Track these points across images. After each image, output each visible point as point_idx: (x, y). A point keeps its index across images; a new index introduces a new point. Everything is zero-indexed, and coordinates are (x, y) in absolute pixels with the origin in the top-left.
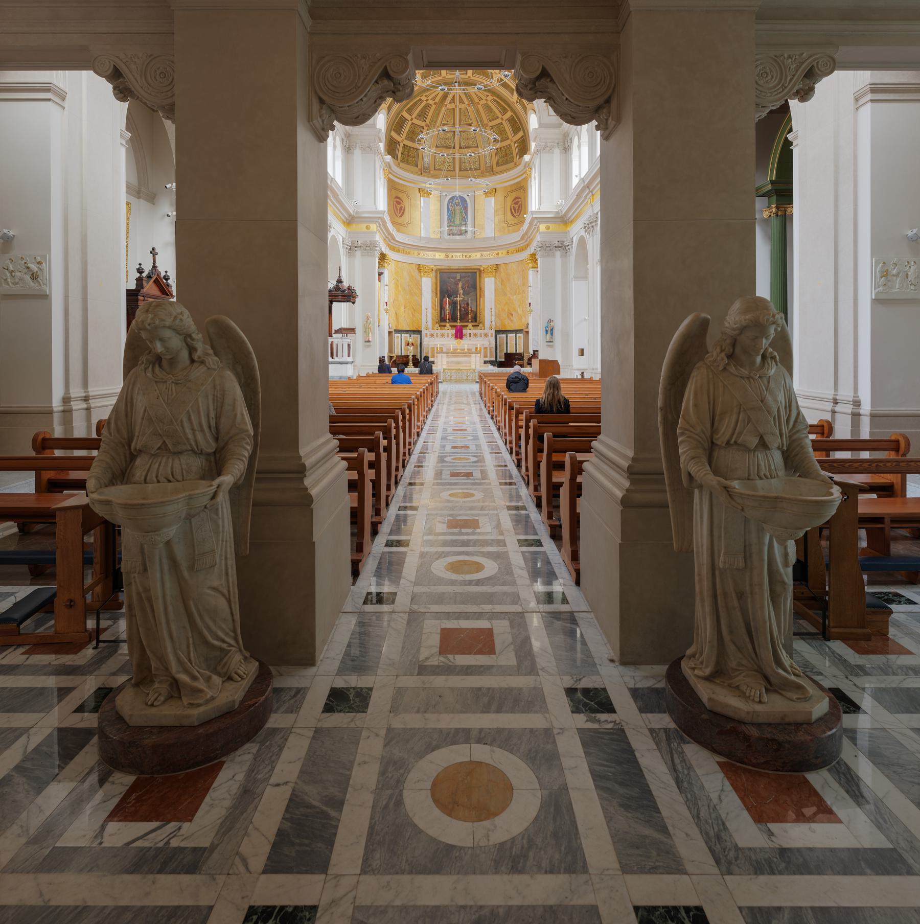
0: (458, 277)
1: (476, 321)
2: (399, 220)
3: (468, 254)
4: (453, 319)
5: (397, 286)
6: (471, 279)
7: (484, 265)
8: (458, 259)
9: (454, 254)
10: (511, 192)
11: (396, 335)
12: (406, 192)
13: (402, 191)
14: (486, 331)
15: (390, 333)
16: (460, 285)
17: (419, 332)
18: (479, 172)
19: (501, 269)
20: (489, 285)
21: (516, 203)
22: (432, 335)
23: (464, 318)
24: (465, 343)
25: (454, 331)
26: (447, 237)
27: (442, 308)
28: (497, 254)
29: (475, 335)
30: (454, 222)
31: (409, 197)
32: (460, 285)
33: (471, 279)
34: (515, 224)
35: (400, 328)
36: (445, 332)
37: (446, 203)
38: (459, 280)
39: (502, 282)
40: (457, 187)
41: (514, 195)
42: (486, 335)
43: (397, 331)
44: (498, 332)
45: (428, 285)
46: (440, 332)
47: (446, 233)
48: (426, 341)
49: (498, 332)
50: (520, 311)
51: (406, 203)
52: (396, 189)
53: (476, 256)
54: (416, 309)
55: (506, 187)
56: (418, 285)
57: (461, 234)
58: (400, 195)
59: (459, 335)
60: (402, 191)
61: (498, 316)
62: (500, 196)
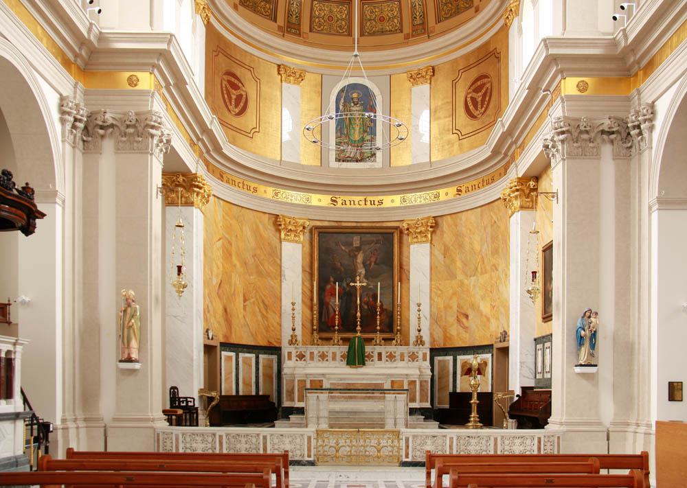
0: (356, 241)
1: (391, 330)
2: (235, 121)
3: (377, 198)
4: (348, 324)
5: (227, 254)
6: (384, 245)
7: (410, 218)
8: (356, 210)
9: (347, 198)
10: (468, 68)
12: (250, 69)
13: (242, 64)
14: (412, 348)
15: (209, 349)
16: (360, 259)
17: (275, 350)
18: (401, 35)
19: (445, 225)
20: (419, 258)
21: (477, 90)
22: (301, 357)
23: (368, 325)
24: (374, 371)
25: (345, 349)
26: (334, 164)
27: (322, 304)
28: (437, 196)
29: (391, 357)
30: (348, 136)
31: (257, 80)
32: (360, 259)
33: (384, 245)
34: (475, 132)
35: (234, 340)
36: (329, 349)
37: (333, 98)
38: (358, 249)
39: (446, 252)
40: (356, 66)
41: (474, 74)
42: (413, 357)
43: (226, 346)
44: (435, 352)
45: (294, 255)
46: (316, 350)
47: (333, 155)
48: (289, 366)
49: (435, 352)
50: (485, 308)
51: (250, 89)
52: (229, 56)
53: (392, 201)
54: (270, 304)
55: (455, 61)
56: (275, 256)
57: (361, 160)
58: (239, 72)
59: (356, 358)
60: (242, 64)
61: (435, 320)
62: (443, 83)
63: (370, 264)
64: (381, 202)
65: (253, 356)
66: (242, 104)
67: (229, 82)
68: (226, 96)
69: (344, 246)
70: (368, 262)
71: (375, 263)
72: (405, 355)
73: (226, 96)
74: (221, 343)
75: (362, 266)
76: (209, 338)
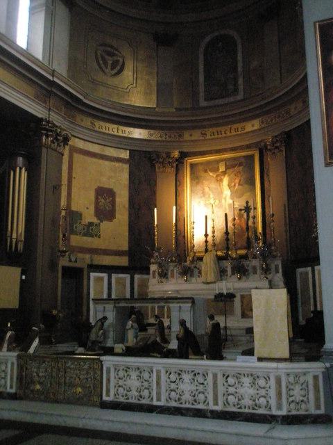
0: (222, 168)
11: (92, 275)
28: (287, 113)
63: (235, 185)
64: (243, 128)
65: (127, 277)
66: (119, 67)
67: (105, 51)
68: (101, 62)
69: (211, 172)
70: (233, 184)
71: (239, 185)
72: (258, 268)
73: (101, 62)
74: (88, 265)
75: (227, 187)
76: (70, 261)
